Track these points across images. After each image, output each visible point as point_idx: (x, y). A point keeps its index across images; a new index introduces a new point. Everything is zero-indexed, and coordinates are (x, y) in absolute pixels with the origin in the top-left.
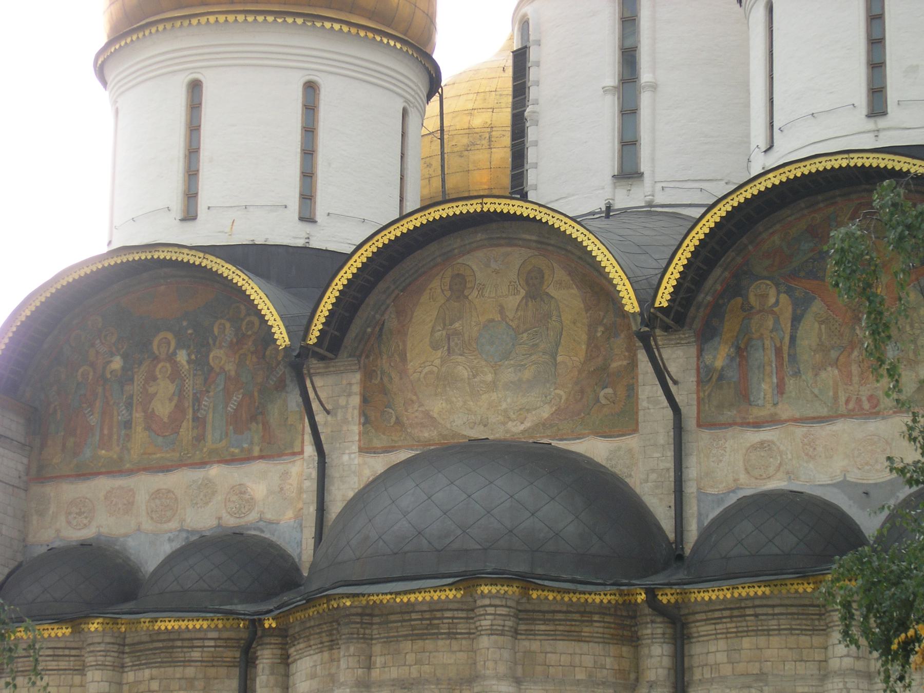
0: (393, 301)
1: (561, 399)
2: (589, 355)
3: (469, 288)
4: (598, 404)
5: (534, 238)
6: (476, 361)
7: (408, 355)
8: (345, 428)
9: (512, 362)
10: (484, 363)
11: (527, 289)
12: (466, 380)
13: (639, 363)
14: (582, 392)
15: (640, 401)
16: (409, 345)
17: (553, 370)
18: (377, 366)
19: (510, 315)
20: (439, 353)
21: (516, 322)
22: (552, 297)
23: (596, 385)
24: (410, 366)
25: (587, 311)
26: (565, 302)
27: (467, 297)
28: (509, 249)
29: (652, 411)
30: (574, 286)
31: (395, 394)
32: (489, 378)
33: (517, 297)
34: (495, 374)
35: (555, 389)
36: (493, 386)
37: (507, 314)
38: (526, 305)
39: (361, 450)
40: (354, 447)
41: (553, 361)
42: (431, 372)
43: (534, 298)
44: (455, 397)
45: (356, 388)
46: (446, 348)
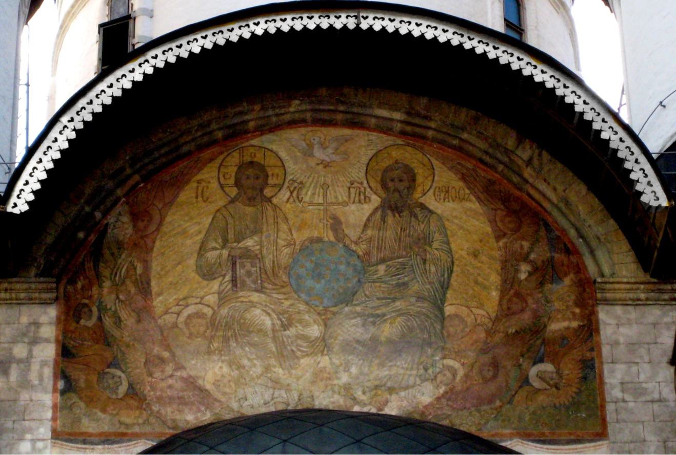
0: (126, 195)
1: (454, 375)
2: (505, 307)
3: (274, 186)
4: (527, 388)
5: (397, 116)
6: (287, 303)
7: (153, 283)
8: (25, 396)
9: (358, 309)
10: (302, 307)
11: (383, 195)
12: (270, 333)
13: (602, 327)
14: (495, 365)
15: (607, 387)
16: (155, 266)
17: (438, 327)
18: (90, 297)
19: (352, 233)
20: (215, 285)
21: (364, 247)
22: (431, 212)
23: (522, 356)
24: (158, 303)
25: (498, 238)
26: (456, 221)
27: (269, 200)
28: (347, 132)
29: (631, 405)
30: (474, 199)
31: (128, 346)
32: (315, 331)
33: (366, 206)
34: (326, 325)
35: (444, 358)
36: (322, 345)
37: (347, 232)
38: (383, 219)
39: (57, 435)
40: (42, 430)
41: (437, 313)
42: (199, 315)
43: (396, 209)
44: (249, 359)
45: (49, 331)
46: (228, 278)
